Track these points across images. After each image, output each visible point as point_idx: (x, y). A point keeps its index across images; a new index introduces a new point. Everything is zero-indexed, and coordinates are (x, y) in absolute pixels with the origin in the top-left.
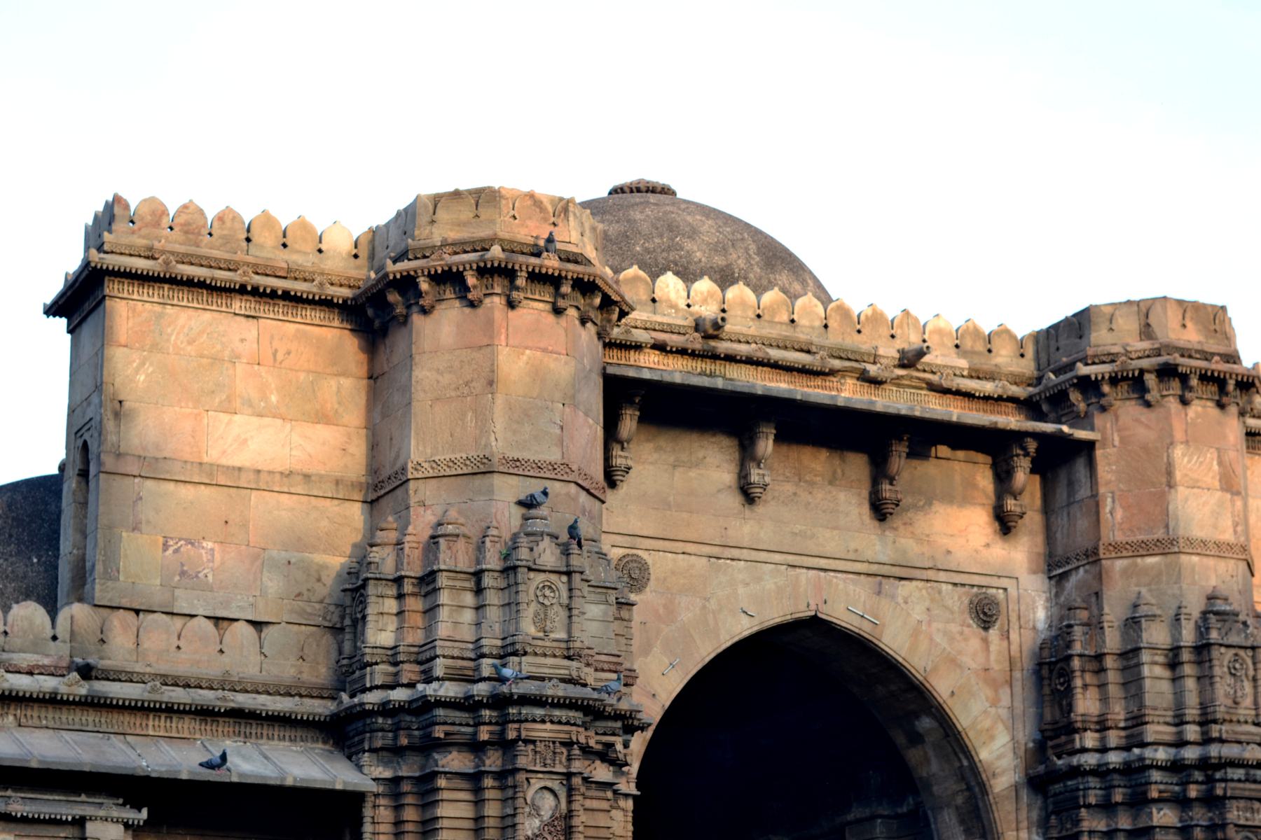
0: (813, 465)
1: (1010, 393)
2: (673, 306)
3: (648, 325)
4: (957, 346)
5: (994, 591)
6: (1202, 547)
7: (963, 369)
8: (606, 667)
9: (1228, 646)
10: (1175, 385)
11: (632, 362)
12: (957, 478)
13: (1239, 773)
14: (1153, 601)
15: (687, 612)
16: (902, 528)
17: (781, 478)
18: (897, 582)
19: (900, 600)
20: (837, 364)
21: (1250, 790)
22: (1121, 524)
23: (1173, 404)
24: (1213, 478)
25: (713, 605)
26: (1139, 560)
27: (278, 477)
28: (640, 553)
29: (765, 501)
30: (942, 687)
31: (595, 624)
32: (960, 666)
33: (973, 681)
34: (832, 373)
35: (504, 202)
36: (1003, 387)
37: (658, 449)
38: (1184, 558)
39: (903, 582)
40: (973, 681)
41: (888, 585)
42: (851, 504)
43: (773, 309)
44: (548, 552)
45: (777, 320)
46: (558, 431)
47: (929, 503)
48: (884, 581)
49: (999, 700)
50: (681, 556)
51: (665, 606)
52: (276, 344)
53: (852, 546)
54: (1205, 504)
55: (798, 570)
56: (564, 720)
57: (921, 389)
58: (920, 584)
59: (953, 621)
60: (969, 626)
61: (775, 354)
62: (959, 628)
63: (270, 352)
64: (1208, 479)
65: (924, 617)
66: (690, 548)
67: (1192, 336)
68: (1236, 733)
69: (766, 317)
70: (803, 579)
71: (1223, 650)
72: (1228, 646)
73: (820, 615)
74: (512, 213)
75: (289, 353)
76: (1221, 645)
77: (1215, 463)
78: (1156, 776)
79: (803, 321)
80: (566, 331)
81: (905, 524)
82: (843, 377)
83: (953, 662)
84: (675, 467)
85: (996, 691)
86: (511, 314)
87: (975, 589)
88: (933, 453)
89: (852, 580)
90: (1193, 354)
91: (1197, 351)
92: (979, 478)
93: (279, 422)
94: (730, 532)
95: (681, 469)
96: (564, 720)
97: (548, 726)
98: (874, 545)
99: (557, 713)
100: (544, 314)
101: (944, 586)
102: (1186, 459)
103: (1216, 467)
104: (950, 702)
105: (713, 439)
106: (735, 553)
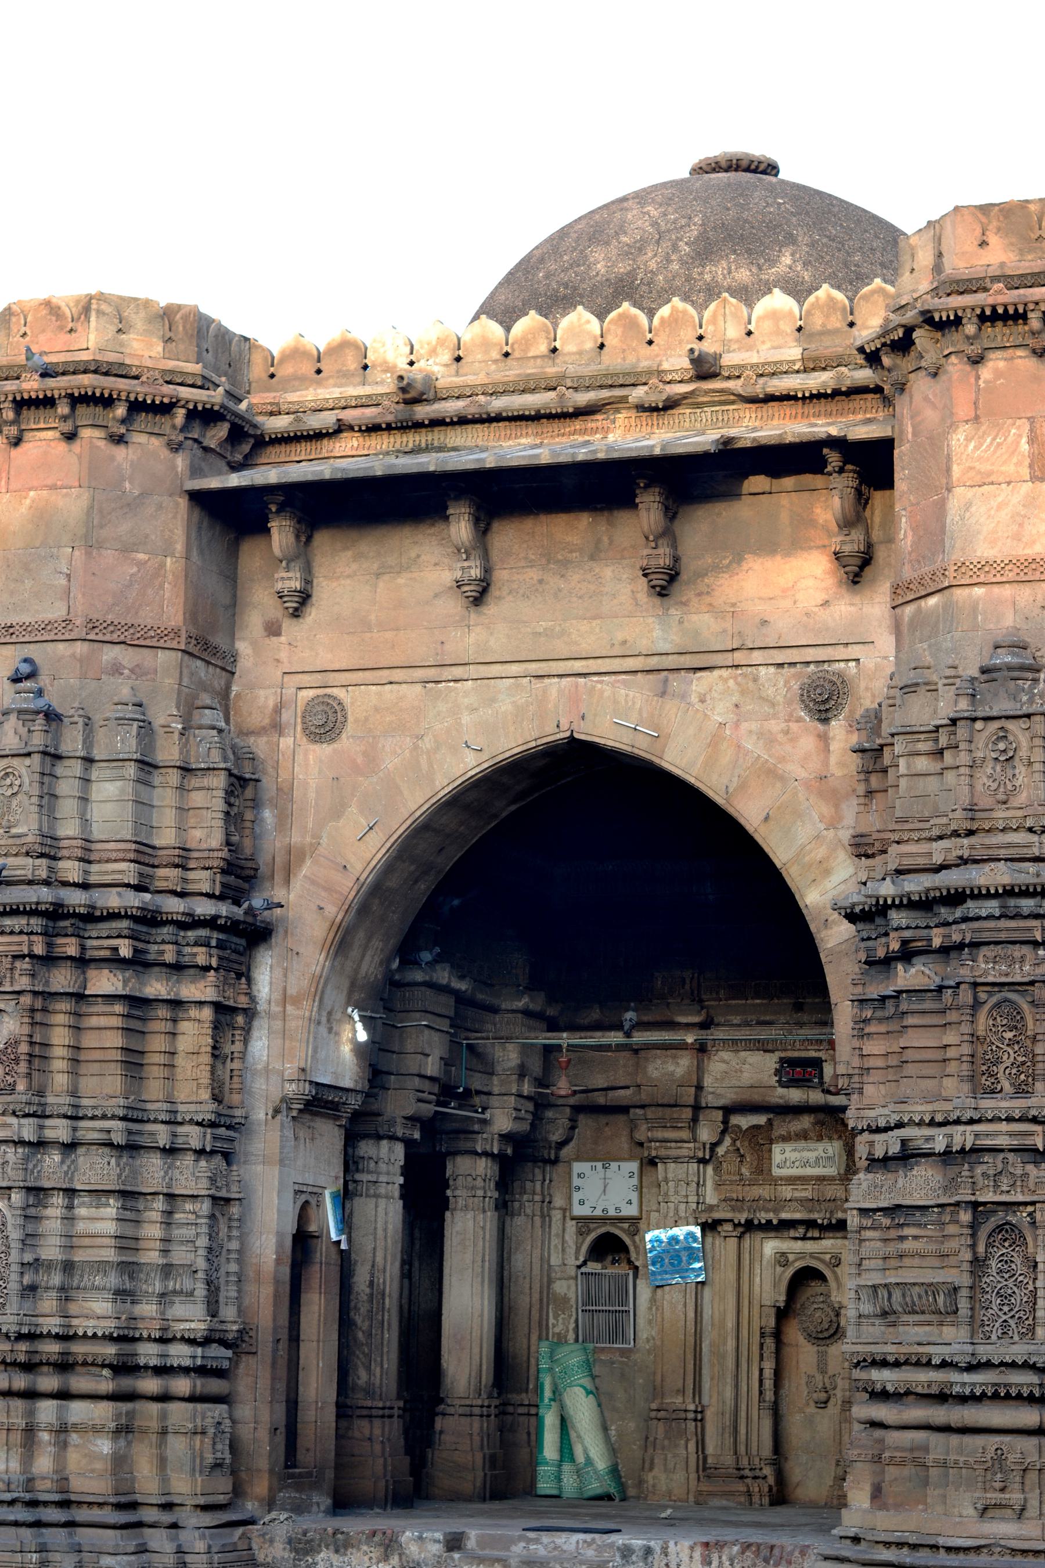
0: (569, 539)
1: (848, 383)
3: (343, 403)
4: (800, 329)
5: (842, 665)
6: (987, 573)
7: (794, 362)
8: (114, 855)
9: (987, 719)
10: (954, 341)
12: (784, 517)
13: (992, 906)
14: (928, 660)
15: (393, 755)
17: (523, 564)
18: (691, 675)
19: (694, 699)
20: (583, 398)
21: (1007, 929)
22: (910, 553)
23: (956, 367)
24: (1019, 464)
25: (427, 743)
26: (922, 602)
28: (335, 692)
30: (749, 813)
31: (109, 805)
32: (782, 778)
33: (801, 796)
35: (14, 319)
36: (839, 378)
38: (958, 592)
39: (699, 674)
41: (675, 682)
42: (619, 584)
43: (526, 341)
44: (11, 733)
45: (530, 354)
46: (63, 582)
47: (739, 559)
48: (671, 676)
49: (841, 818)
50: (388, 687)
51: (365, 754)
53: (620, 636)
54: (999, 508)
55: (546, 681)
56: (17, 929)
57: (733, 403)
58: (724, 673)
59: (775, 716)
60: (799, 720)
61: (498, 404)
62: (783, 725)
64: (1010, 468)
66: (398, 675)
67: (999, 255)
68: (989, 847)
69: (517, 354)
70: (554, 692)
71: (979, 725)
72: (987, 719)
73: (576, 735)
74: (23, 330)
76: (974, 720)
77: (1024, 440)
78: (897, 918)
80: (80, 457)
81: (700, 594)
82: (617, 411)
83: (771, 773)
84: (378, 575)
85: (837, 806)
86: (15, 452)
87: (812, 666)
88: (744, 491)
91: (995, 279)
92: (818, 511)
94: (447, 647)
95: (386, 577)
96: (17, 929)
98: (650, 631)
101: (763, 670)
103: (1024, 446)
104: (762, 830)
105: (432, 531)
106: (458, 672)
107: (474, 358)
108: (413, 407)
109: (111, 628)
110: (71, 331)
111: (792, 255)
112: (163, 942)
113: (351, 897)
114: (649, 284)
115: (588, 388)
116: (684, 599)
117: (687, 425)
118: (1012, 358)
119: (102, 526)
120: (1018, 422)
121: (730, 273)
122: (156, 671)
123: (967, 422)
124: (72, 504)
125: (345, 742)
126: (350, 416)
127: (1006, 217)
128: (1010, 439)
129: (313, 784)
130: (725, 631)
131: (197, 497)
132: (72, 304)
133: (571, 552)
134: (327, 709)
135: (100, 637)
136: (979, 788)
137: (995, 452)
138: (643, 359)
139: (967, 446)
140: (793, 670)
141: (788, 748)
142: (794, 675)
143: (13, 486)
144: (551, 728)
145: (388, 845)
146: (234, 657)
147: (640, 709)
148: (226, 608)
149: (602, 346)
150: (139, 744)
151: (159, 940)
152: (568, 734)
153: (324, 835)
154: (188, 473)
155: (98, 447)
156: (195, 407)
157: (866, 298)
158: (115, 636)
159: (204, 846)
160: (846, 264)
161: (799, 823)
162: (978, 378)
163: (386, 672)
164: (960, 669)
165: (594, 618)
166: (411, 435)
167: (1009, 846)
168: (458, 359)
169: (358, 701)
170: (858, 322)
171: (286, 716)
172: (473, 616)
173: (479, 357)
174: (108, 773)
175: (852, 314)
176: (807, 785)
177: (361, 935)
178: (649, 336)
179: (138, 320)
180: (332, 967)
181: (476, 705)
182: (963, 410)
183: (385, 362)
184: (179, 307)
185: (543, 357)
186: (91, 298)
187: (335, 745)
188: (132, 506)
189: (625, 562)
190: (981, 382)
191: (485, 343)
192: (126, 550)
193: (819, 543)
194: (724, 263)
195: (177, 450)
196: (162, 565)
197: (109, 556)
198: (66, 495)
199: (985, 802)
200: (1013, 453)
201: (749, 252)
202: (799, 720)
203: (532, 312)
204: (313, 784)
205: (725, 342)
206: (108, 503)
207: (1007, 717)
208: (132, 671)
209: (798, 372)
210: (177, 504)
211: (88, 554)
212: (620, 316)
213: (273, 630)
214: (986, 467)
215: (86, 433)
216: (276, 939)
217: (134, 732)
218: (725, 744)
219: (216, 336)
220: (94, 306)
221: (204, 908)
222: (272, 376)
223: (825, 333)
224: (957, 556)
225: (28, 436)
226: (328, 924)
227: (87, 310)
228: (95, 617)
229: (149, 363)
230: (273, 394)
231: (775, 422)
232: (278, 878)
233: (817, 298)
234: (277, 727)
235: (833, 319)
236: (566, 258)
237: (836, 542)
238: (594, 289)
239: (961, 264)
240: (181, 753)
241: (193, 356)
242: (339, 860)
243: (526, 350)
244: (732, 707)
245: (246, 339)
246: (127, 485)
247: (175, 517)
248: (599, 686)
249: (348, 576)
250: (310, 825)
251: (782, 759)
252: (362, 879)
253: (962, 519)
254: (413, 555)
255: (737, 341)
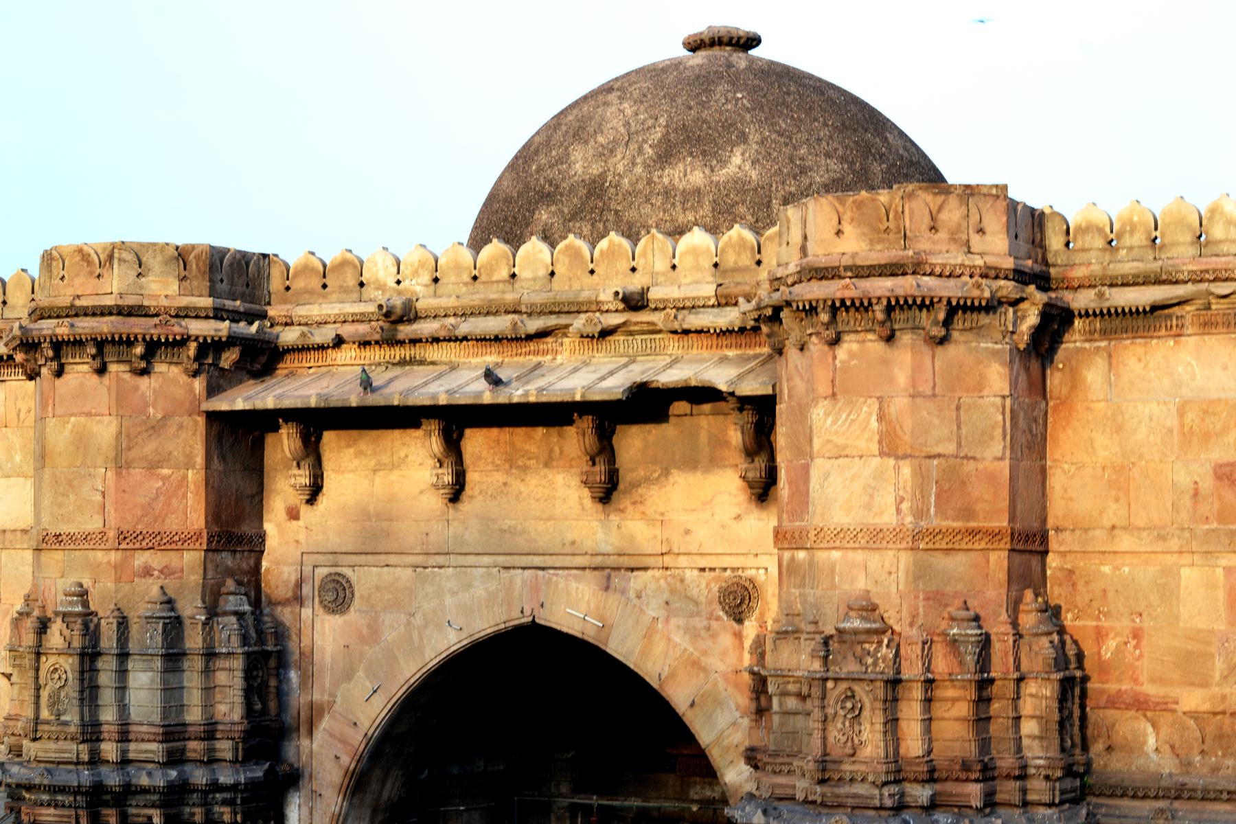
2: (382, 287)
4: (716, 265)
7: (709, 298)
8: (146, 737)
11: (329, 362)
12: (703, 437)
15: (392, 628)
16: (630, 509)
17: (490, 467)
19: (632, 594)
20: (534, 325)
23: (816, 346)
24: (870, 440)
25: (418, 620)
27: (19, 533)
29: (472, 497)
30: (679, 696)
32: (704, 670)
34: (542, 334)
35: (54, 264)
37: (359, 454)
39: (635, 573)
40: (721, 685)
43: (491, 267)
45: (495, 278)
46: (99, 498)
47: (666, 473)
48: (613, 574)
50: (386, 569)
51: (369, 626)
52: (20, 404)
54: (853, 479)
55: (512, 571)
58: (657, 573)
59: (698, 614)
60: (718, 619)
61: (465, 328)
62: (705, 623)
63: (14, 413)
64: (862, 444)
65: (662, 613)
68: (838, 796)
69: (483, 278)
70: (518, 581)
73: (537, 620)
75: (29, 411)
77: (874, 418)
79: (523, 272)
80: (109, 389)
81: (634, 503)
83: (696, 665)
84: (375, 471)
86: (58, 382)
89: (575, 576)
90: (843, 273)
91: (846, 268)
93: (22, 480)
95: (381, 473)
97: (52, 811)
98: (595, 534)
99: (60, 798)
100: (87, 376)
102: (829, 421)
103: (874, 424)
107: (448, 279)
108: (395, 325)
109: (140, 537)
110: (99, 276)
111: (743, 154)
112: (194, 804)
113: (361, 749)
114: (616, 187)
115: (541, 313)
116: (622, 507)
117: (622, 350)
118: (864, 341)
119: (129, 449)
120: (869, 401)
121: (685, 175)
122: (182, 570)
123: (825, 398)
124: (105, 430)
125: (353, 615)
126: (347, 330)
127: (858, 208)
128: (863, 415)
129: (329, 650)
130: (655, 537)
131: (213, 417)
132: (100, 252)
133: (529, 459)
134: (337, 586)
135: (131, 546)
136: (831, 740)
137: (849, 427)
138: (584, 288)
139: (825, 421)
140: (713, 574)
141: (709, 643)
142: (714, 579)
143: (58, 412)
144: (516, 613)
145: (389, 706)
146: (262, 537)
147: (589, 601)
148: (252, 497)
149: (552, 274)
150: (165, 639)
151: (191, 802)
152: (530, 619)
153: (339, 695)
154: (205, 394)
155: (124, 380)
156: (205, 338)
157: (770, 238)
158: (144, 543)
159: (227, 719)
160: (791, 160)
161: (719, 710)
162: (835, 358)
163: (383, 557)
164: (820, 624)
165: (550, 519)
166: (397, 349)
167: (855, 796)
168: (436, 280)
169: (364, 579)
170: (765, 261)
171: (306, 590)
172: (451, 511)
173: (453, 279)
174: (139, 665)
175: (759, 252)
176: (725, 677)
177: (378, 772)
178: (591, 266)
179: (154, 262)
180: (351, 805)
181: (456, 589)
182: (823, 388)
183: (378, 280)
184: (193, 247)
185: (504, 282)
186: (114, 246)
187: (346, 617)
188: (156, 428)
189: (573, 471)
190: (837, 362)
191: (458, 267)
192: (152, 466)
193: (733, 462)
194: (681, 166)
195: (194, 376)
196: (185, 477)
197: (137, 473)
198: (99, 421)
199: (836, 752)
200: (864, 429)
201: (704, 153)
202: (718, 619)
203: (495, 241)
204: (329, 650)
205: (653, 274)
206: (137, 429)
207: (853, 680)
208: (161, 572)
209: (713, 306)
210: (196, 422)
211: (119, 474)
212: (567, 247)
213: (293, 514)
214: (841, 441)
215: (113, 368)
216: (303, 783)
217: (160, 631)
218: (658, 636)
219: (231, 265)
220: (116, 255)
221: (226, 777)
222: (288, 288)
223: (737, 270)
224: (817, 521)
225: (68, 368)
226: (342, 773)
227: (111, 257)
228: (125, 527)
229: (164, 302)
230: (288, 306)
231: (695, 351)
232: (303, 730)
233: (730, 238)
234: (298, 599)
235: (744, 257)
236: (554, 153)
237: (743, 464)
238: (572, 189)
239: (821, 252)
240: (204, 640)
241: (206, 291)
242: (350, 717)
243: (490, 275)
244: (663, 604)
245: (265, 256)
246: (151, 410)
247: (194, 434)
248: (555, 578)
249: (352, 471)
250: (327, 685)
251: (705, 653)
252: (370, 734)
253: (822, 487)
254: (402, 454)
255: (664, 274)
